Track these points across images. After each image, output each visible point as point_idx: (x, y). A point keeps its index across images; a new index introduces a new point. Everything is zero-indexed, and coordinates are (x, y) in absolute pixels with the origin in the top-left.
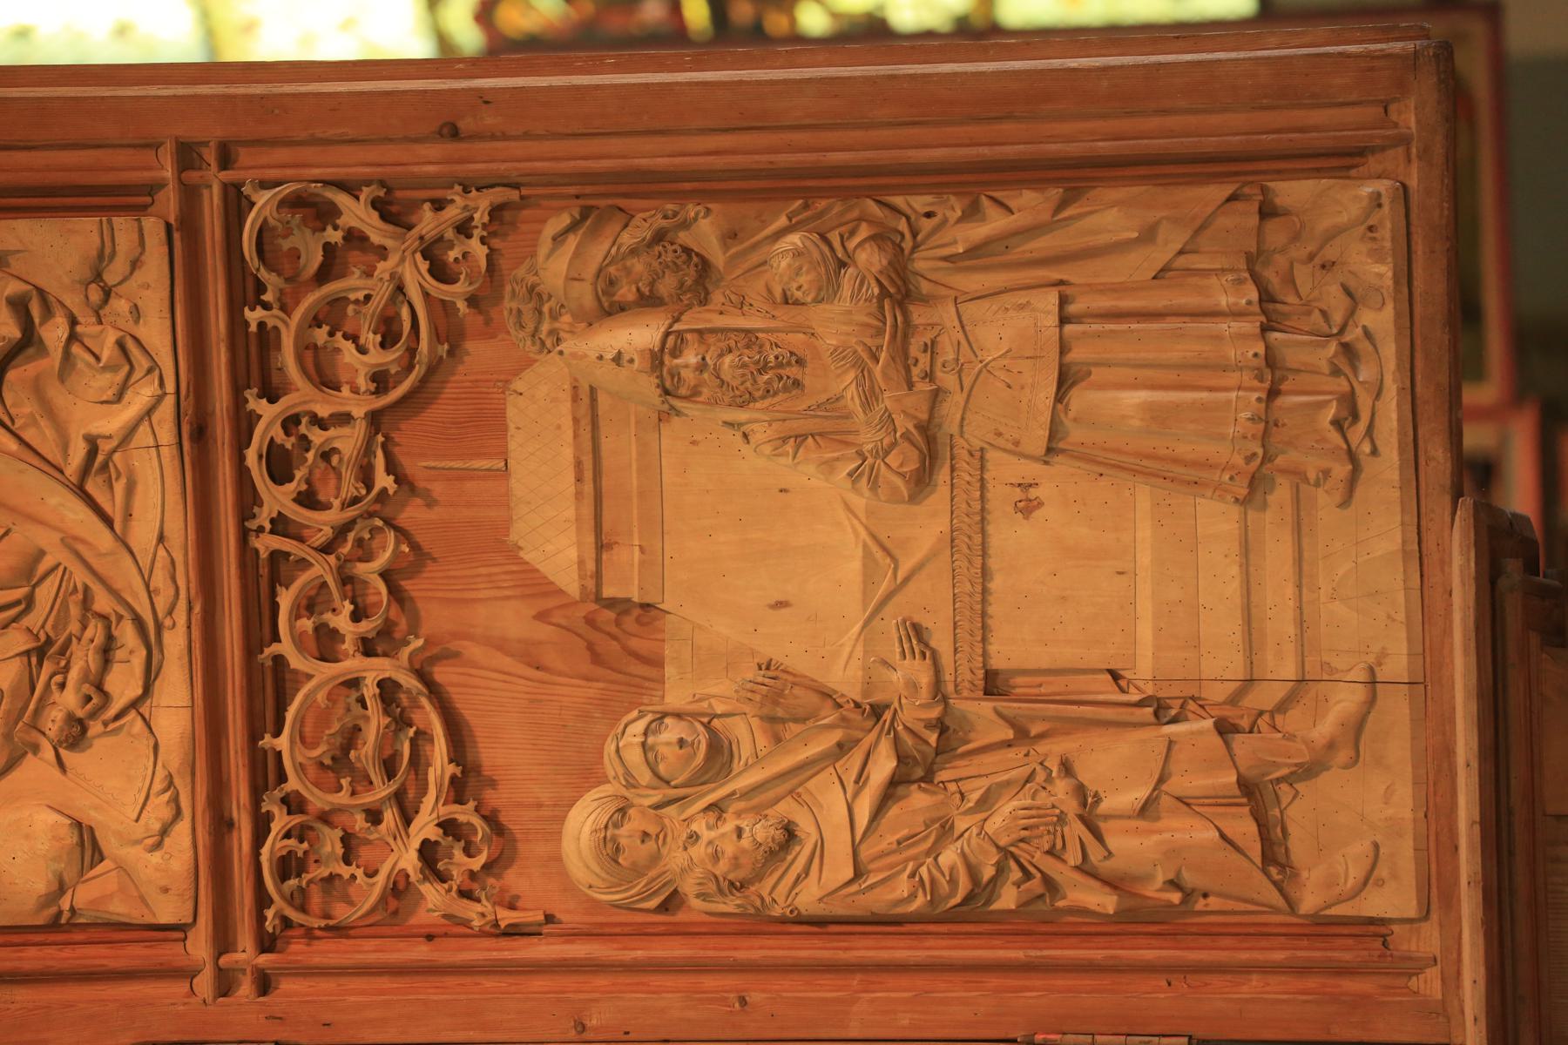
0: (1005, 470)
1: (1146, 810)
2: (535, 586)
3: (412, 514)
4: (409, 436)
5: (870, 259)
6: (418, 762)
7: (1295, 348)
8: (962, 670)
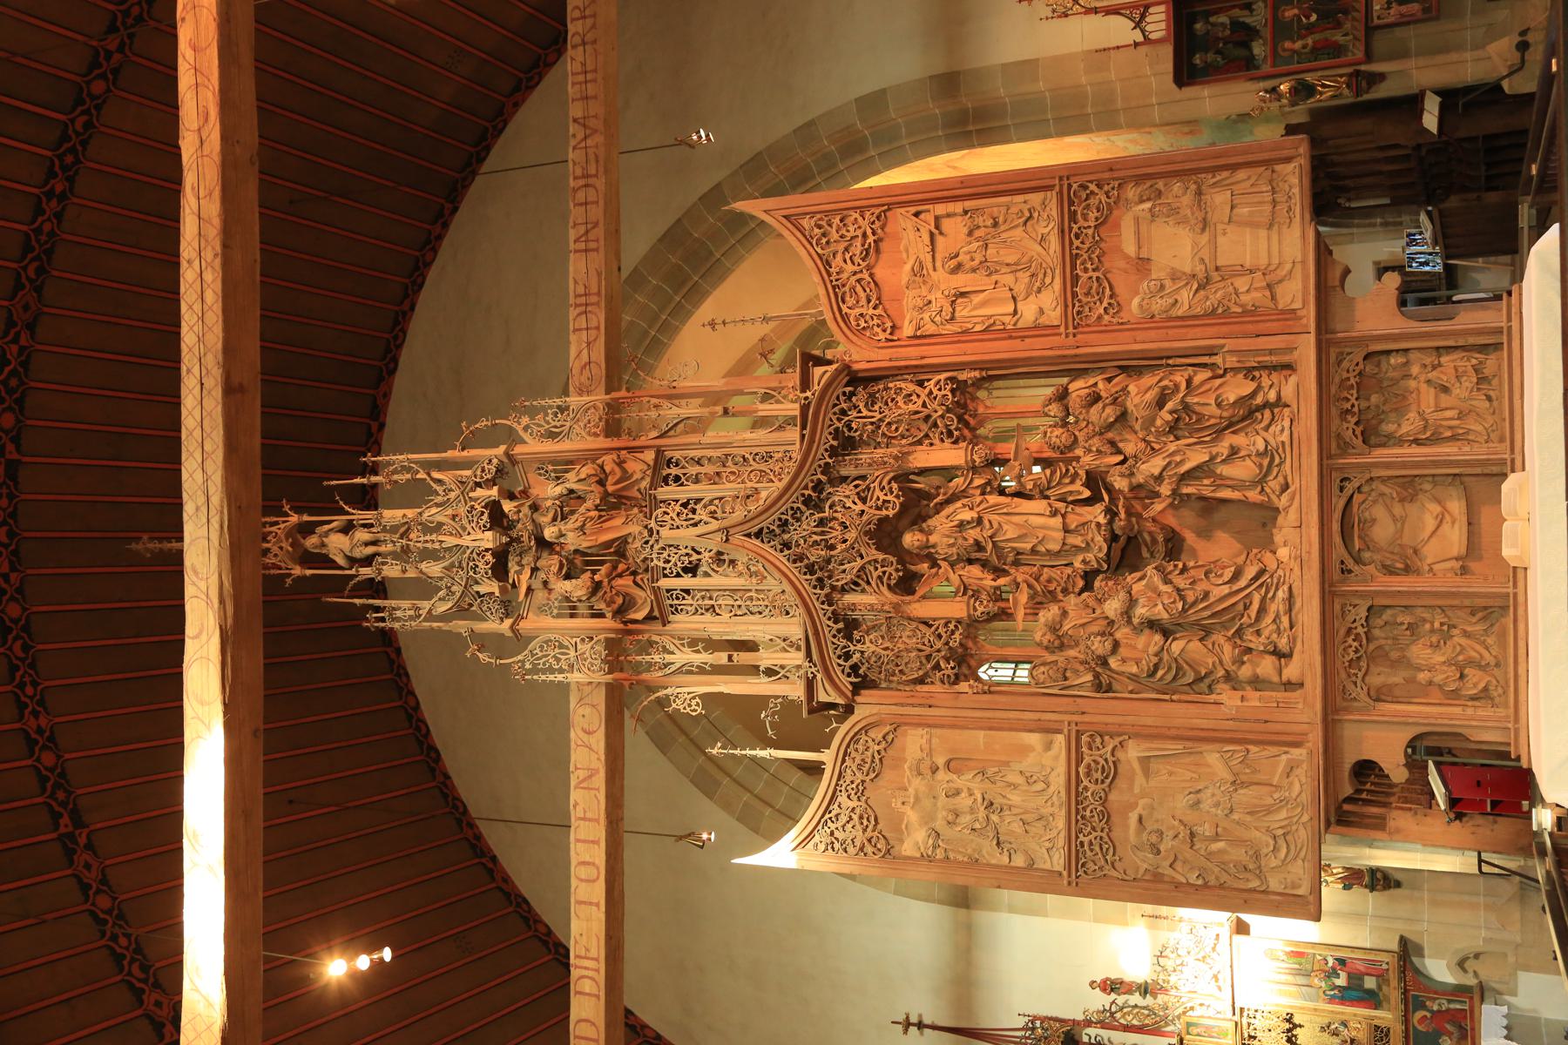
0: (1220, 227)
1: (1248, 291)
2: (1127, 257)
3: (1103, 245)
4: (1102, 229)
5: (1193, 187)
7: (1278, 197)
8: (1211, 267)
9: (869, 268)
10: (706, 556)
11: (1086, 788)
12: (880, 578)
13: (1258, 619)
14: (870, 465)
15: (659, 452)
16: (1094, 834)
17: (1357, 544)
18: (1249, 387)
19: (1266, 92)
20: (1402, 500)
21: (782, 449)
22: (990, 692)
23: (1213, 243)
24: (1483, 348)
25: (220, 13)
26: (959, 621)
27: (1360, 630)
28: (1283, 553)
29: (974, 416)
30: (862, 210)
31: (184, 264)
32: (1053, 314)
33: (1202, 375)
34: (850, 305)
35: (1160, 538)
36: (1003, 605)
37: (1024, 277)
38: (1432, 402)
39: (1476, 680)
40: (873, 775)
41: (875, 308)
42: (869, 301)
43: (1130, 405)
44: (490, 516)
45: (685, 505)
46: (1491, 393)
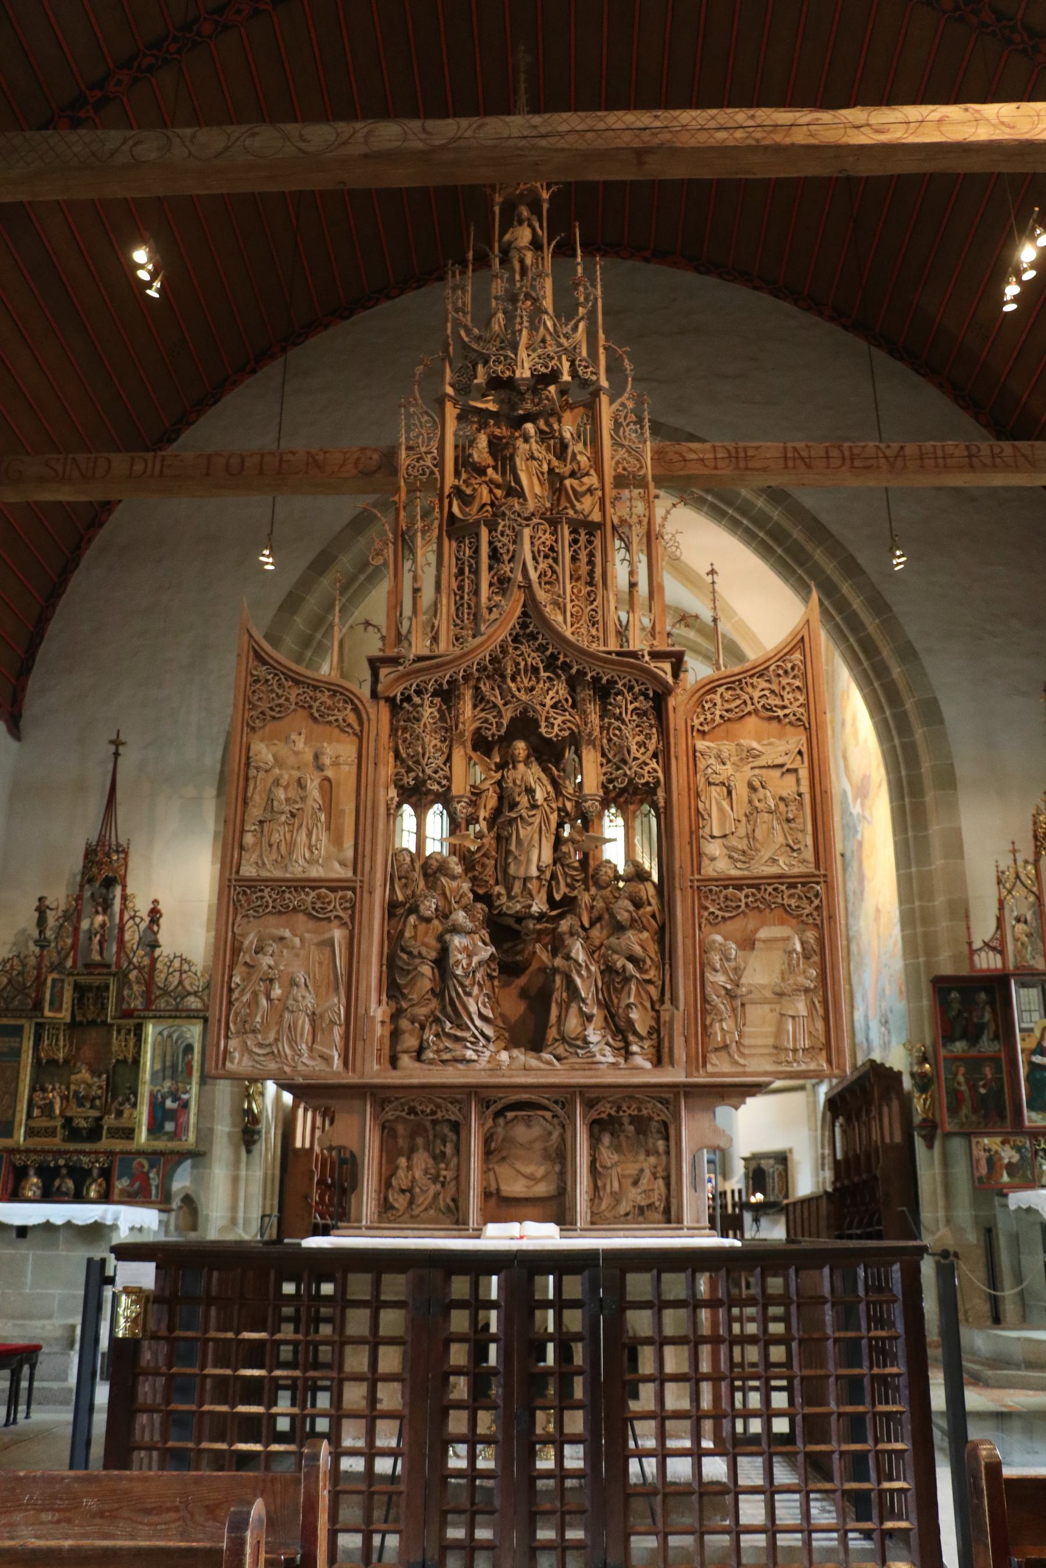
0: (777, 1007)
1: (722, 1029)
2: (756, 930)
4: (781, 910)
8: (745, 1000)
9: (756, 711)
10: (506, 568)
11: (307, 894)
12: (486, 721)
13: (448, 1036)
14: (585, 712)
15: (600, 526)
17: (510, 1115)
18: (642, 1029)
19: (924, 1053)
20: (545, 1149)
21: (601, 635)
22: (388, 815)
23: (765, 1001)
24: (667, 1211)
25: (971, 143)
26: (449, 789)
27: (439, 1115)
28: (504, 1056)
29: (626, 802)
30: (806, 705)
31: (751, 112)
32: (710, 869)
33: (654, 992)
35: (519, 958)
36: (463, 826)
37: (742, 845)
38: (627, 1172)
39: (400, 1202)
40: (317, 715)
41: (721, 717)
42: (727, 711)
43: (630, 934)
44: (544, 374)
45: (552, 549)
46: (630, 1217)
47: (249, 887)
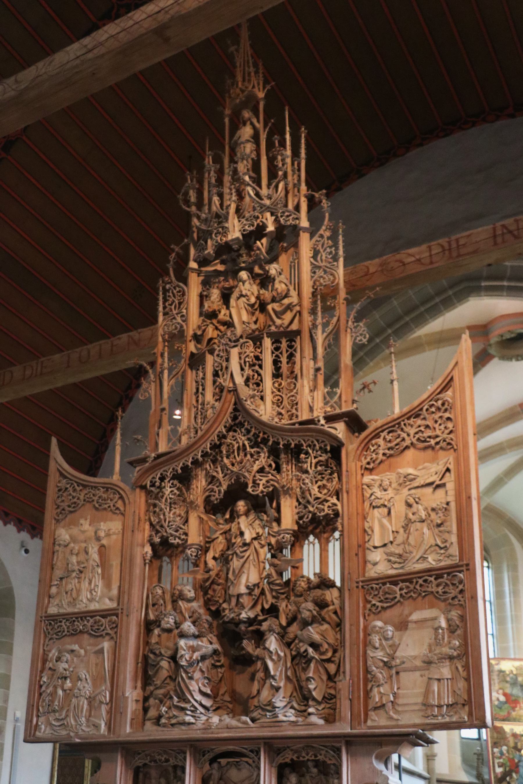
6: (387, 602)
16: (65, 627)
22: (145, 564)
34: (387, 437)
41: (384, 454)
47: (53, 620)
